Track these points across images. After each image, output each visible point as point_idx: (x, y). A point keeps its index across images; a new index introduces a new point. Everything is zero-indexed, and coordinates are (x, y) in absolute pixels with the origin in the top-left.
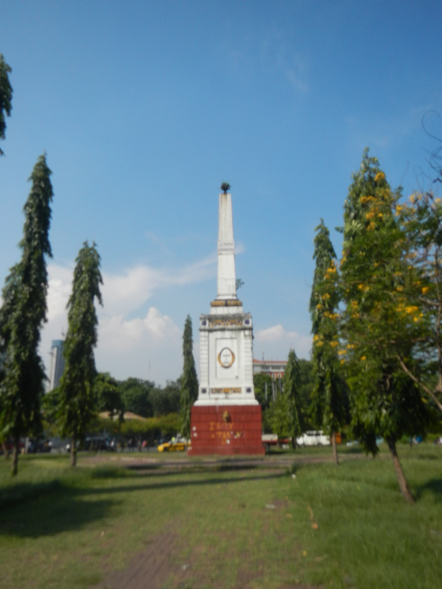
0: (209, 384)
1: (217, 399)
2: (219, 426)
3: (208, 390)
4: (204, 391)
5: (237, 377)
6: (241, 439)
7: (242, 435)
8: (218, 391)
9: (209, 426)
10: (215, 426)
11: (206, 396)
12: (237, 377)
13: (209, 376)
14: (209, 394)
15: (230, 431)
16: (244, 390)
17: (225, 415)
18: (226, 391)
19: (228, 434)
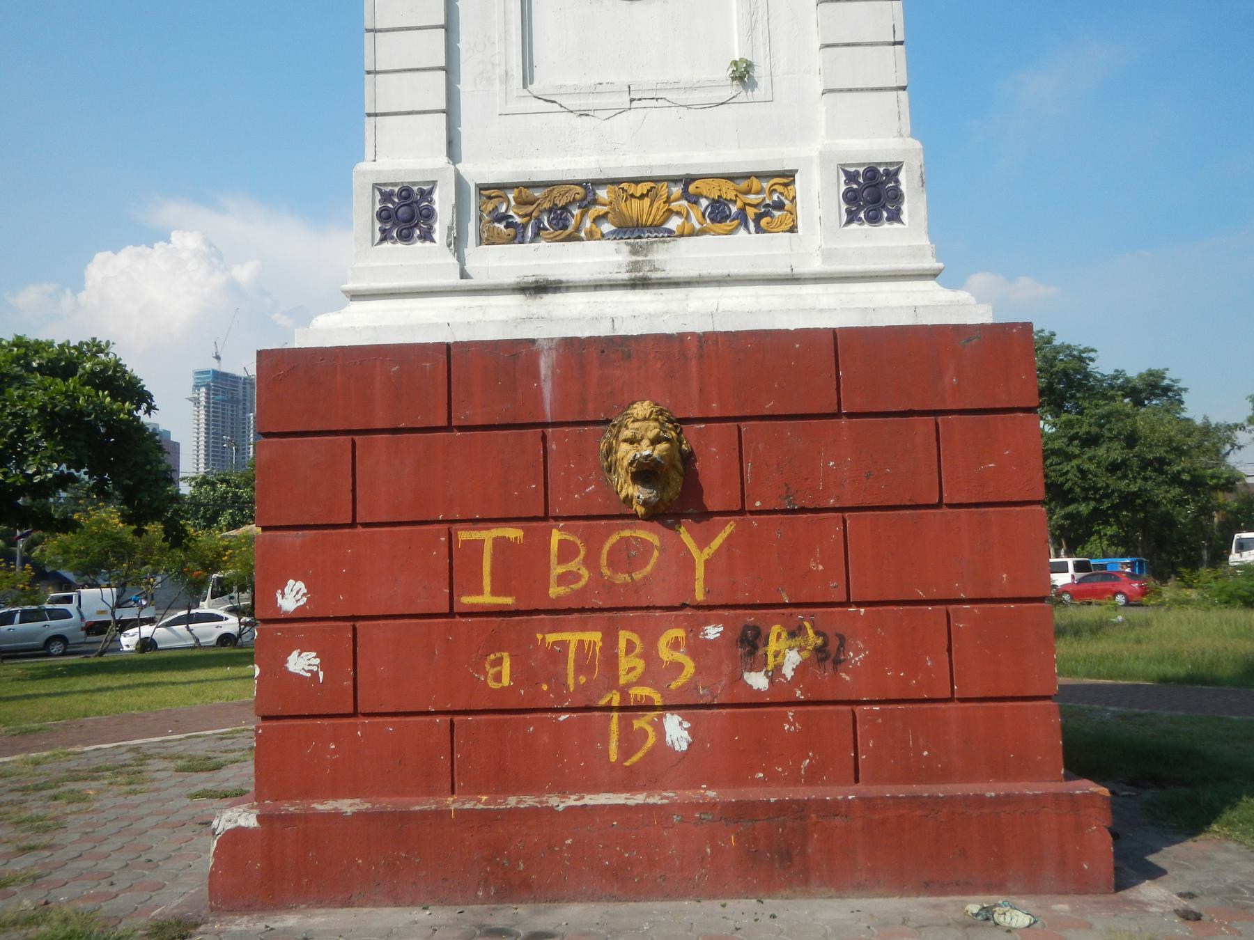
0: (453, 149)
1: (540, 288)
2: (566, 571)
3: (443, 202)
4: (404, 214)
5: (743, 75)
6: (811, 698)
7: (826, 655)
8: (546, 210)
9: (457, 568)
10: (518, 566)
11: (425, 260)
12: (743, 75)
13: (450, 69)
14: (457, 243)
15: (691, 611)
16: (818, 197)
17: (638, 435)
18: (638, 210)
19: (669, 644)
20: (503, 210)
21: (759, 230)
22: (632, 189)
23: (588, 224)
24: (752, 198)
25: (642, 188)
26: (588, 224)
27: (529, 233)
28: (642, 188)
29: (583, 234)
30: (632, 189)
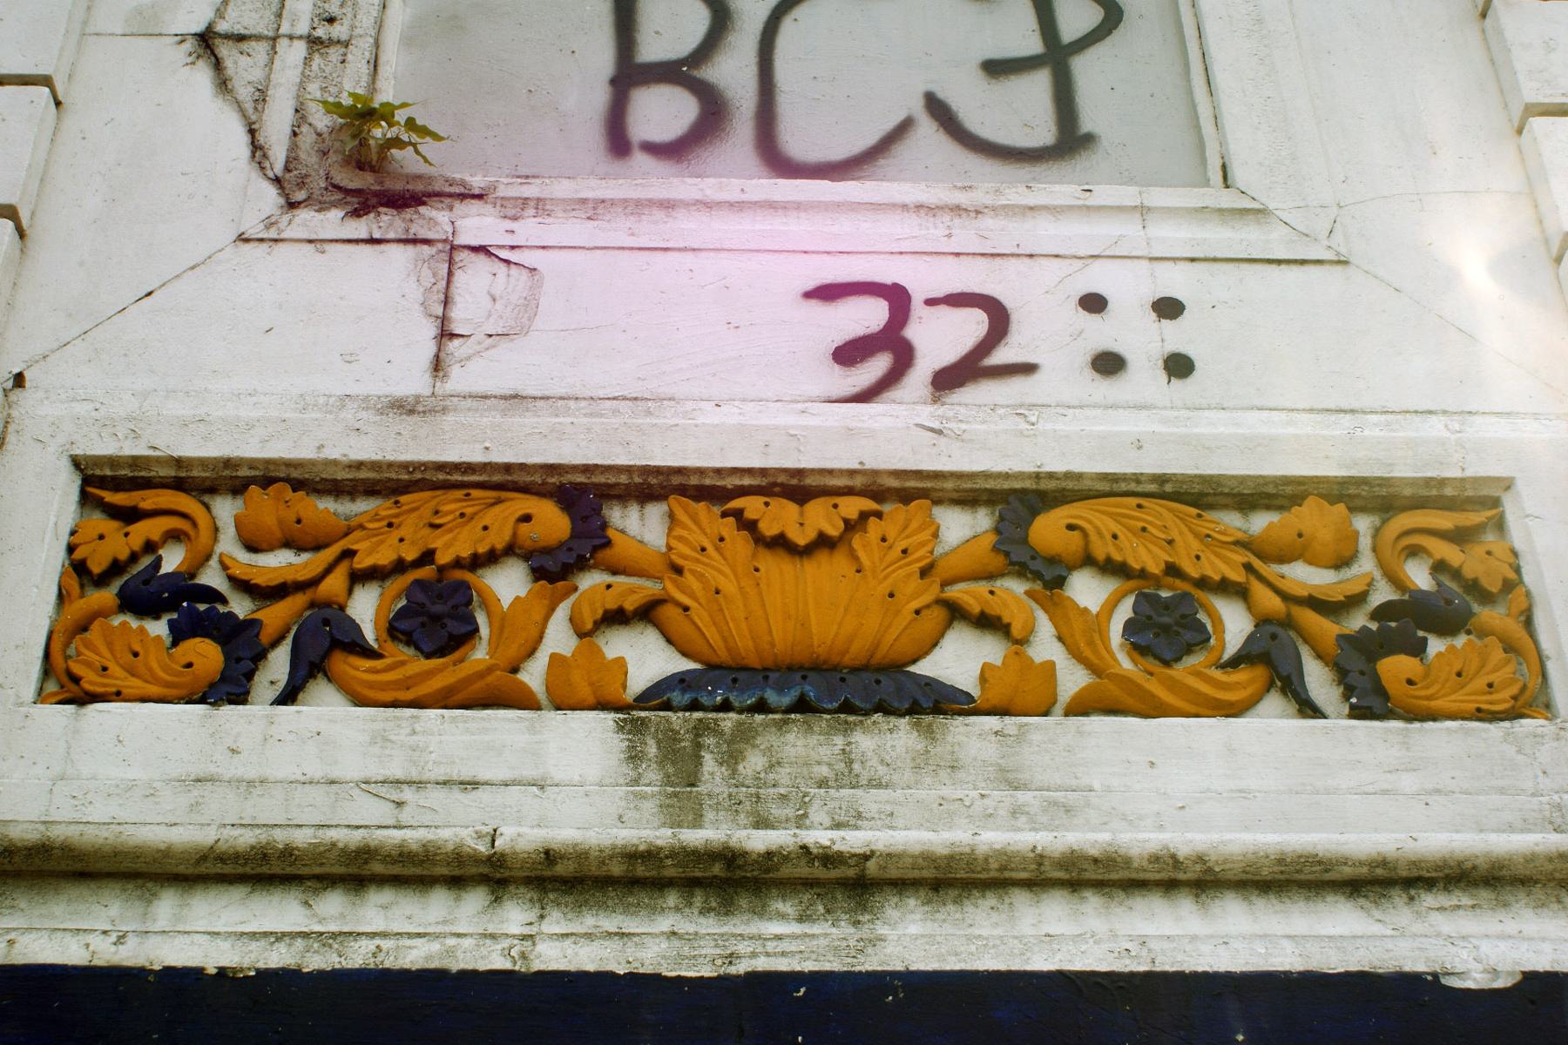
20: (172, 560)
21: (1370, 702)
22: (779, 517)
23: (559, 638)
24: (1305, 576)
25: (821, 518)
26: (559, 638)
27: (278, 665)
28: (821, 518)
29: (533, 676)
30: (779, 517)
